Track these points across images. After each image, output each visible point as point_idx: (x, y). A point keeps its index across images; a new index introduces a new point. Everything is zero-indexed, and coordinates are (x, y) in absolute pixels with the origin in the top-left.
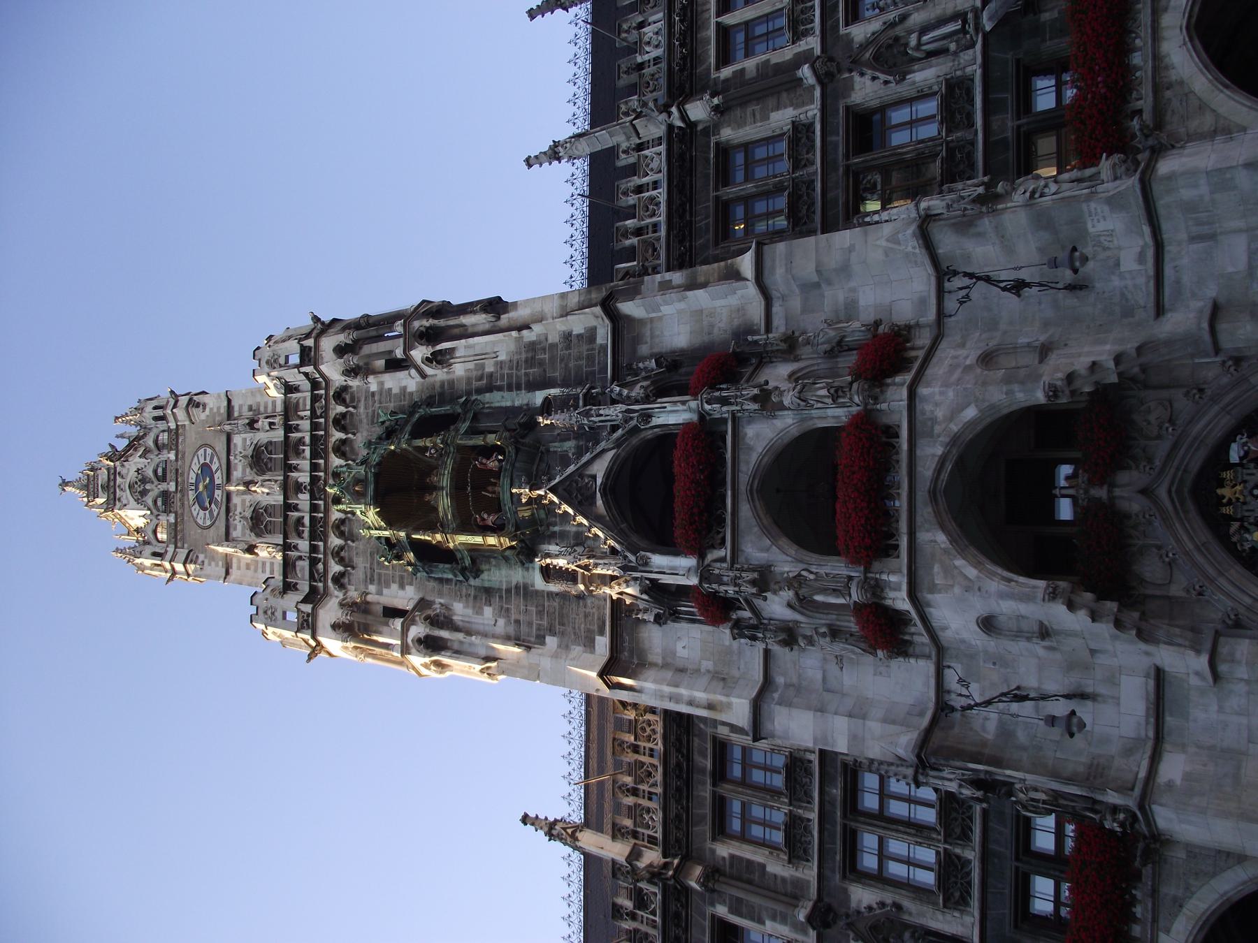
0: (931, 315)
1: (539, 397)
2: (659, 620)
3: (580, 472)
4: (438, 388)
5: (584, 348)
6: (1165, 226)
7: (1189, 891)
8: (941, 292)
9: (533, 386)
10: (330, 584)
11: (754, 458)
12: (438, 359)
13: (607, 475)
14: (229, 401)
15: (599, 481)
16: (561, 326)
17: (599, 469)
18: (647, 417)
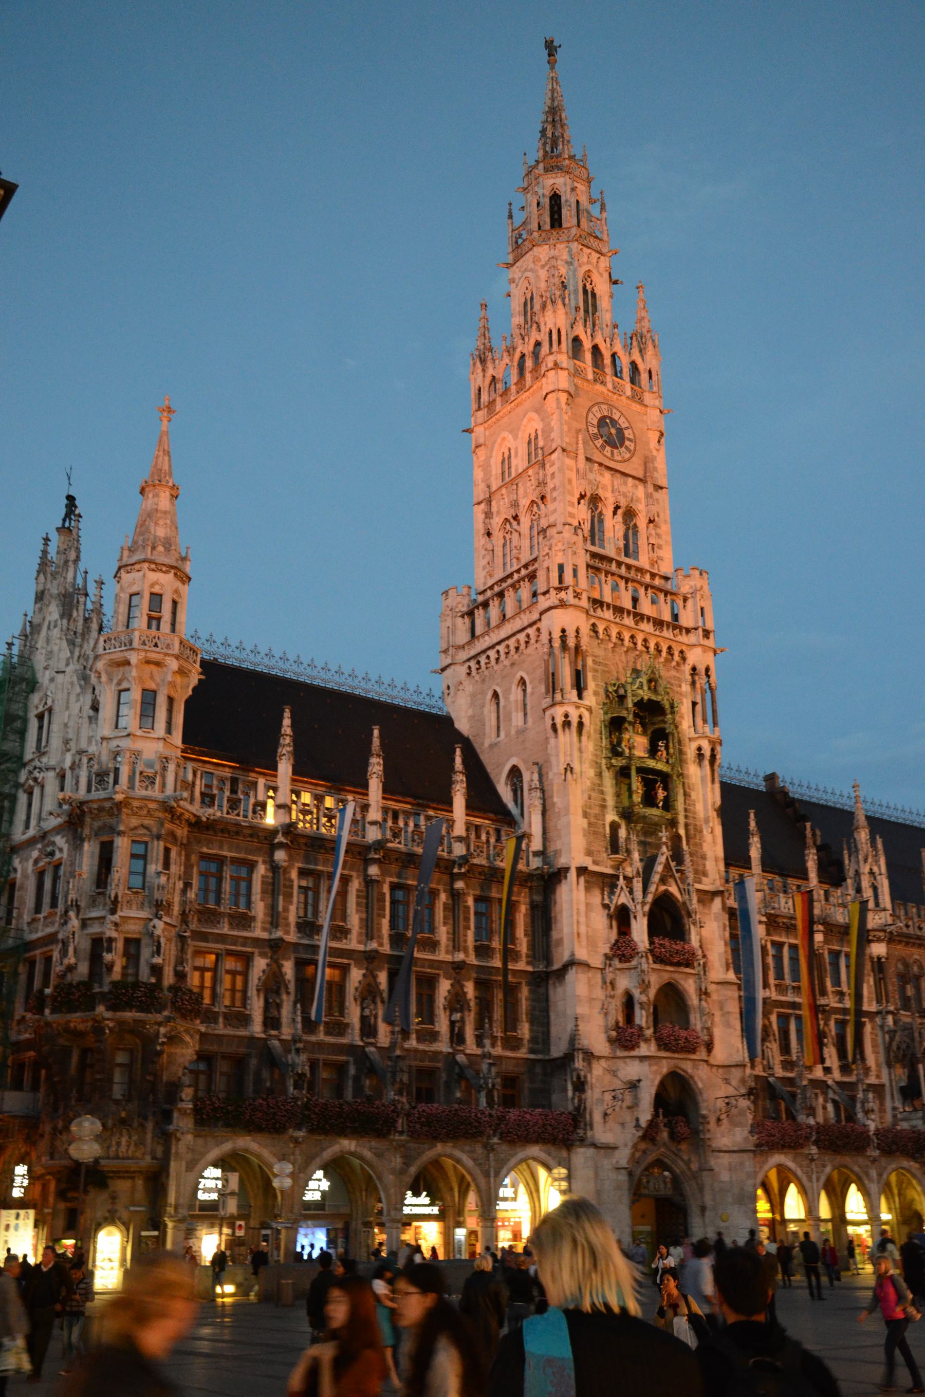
0: (712, 1061)
1: (682, 832)
2: (606, 906)
3: (673, 876)
4: (684, 749)
5: (700, 868)
6: (735, 1155)
7: (554, 1158)
8: (718, 1066)
9: (686, 826)
10: (593, 621)
11: (682, 982)
12: (700, 756)
13: (672, 894)
14: (661, 488)
15: (670, 889)
16: (710, 854)
17: (673, 889)
18: (694, 924)
